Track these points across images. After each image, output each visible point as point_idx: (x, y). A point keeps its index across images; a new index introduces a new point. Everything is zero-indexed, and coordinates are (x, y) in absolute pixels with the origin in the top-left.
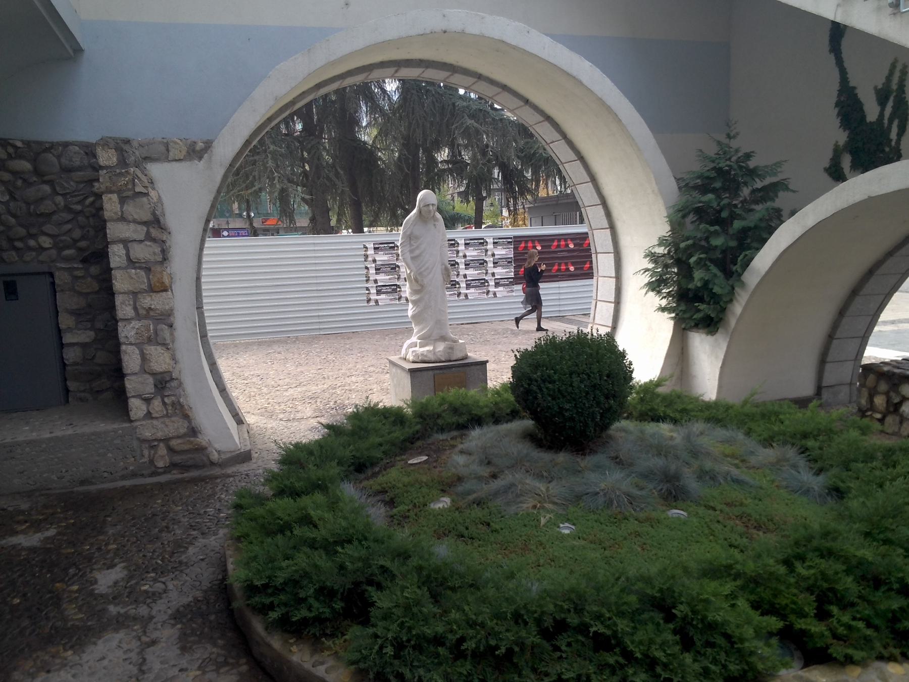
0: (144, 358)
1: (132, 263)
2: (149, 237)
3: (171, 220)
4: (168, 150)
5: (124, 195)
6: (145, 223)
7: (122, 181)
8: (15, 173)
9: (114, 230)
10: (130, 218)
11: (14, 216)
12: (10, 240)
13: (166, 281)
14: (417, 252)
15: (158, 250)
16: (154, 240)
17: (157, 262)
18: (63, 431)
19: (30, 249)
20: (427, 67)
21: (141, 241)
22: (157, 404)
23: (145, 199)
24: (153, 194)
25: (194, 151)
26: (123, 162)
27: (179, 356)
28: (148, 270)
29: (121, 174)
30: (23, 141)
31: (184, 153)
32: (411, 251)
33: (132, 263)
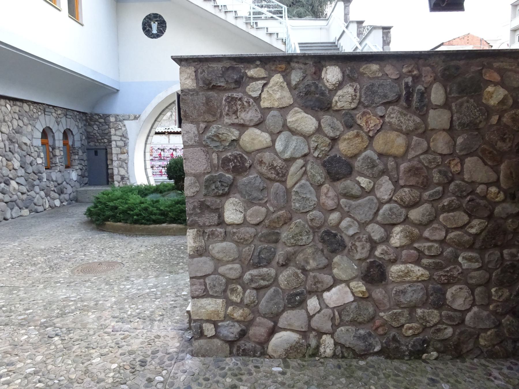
0: (119, 171)
1: (117, 146)
2: (121, 140)
3: (129, 136)
7: (116, 125)
8: (100, 123)
9: (113, 138)
12: (98, 140)
13: (125, 151)
15: (123, 143)
18: (98, 188)
19: (102, 142)
22: (121, 183)
24: (123, 129)
26: (116, 121)
27: (129, 171)
28: (121, 148)
33: (117, 146)
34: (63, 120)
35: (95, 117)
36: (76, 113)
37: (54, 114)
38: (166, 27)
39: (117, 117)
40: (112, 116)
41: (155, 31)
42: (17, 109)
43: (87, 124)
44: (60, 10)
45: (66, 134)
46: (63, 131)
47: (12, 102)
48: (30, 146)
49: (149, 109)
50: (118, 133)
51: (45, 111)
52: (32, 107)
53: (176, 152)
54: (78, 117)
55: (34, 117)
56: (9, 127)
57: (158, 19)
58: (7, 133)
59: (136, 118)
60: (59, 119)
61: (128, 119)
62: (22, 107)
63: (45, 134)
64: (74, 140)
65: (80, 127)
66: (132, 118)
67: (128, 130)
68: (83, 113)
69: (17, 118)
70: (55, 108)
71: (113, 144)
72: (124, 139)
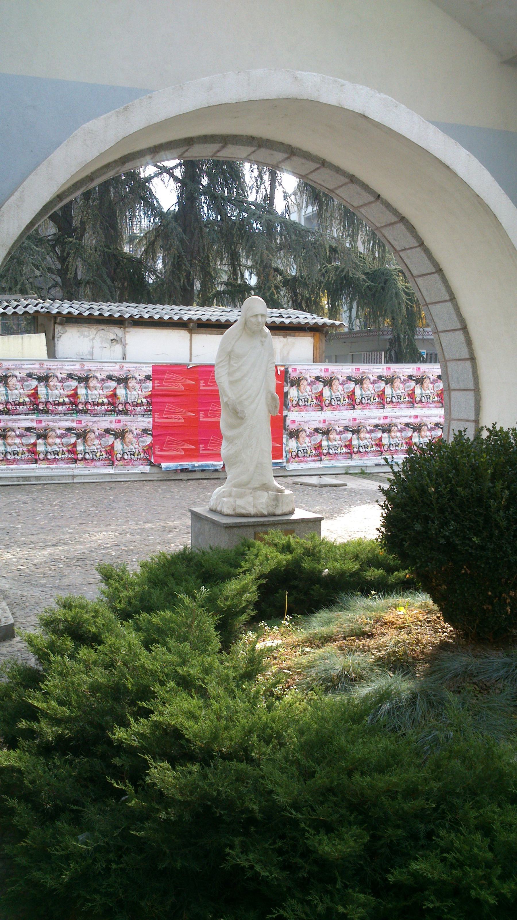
20: (259, 146)
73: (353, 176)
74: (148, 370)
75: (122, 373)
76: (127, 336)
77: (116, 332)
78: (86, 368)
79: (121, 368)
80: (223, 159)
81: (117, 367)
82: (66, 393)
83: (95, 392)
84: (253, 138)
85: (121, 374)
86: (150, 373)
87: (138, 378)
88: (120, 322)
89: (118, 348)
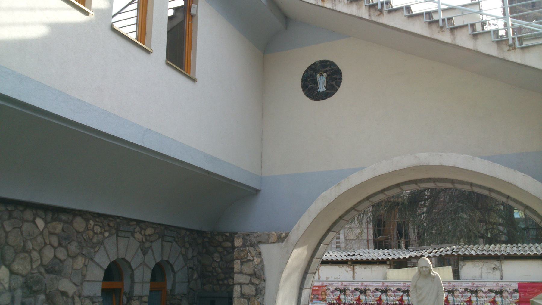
1: (243, 295)
2: (251, 282)
4: (269, 238)
5: (243, 260)
6: (250, 275)
7: (243, 254)
8: (225, 248)
9: (238, 278)
10: (244, 272)
11: (221, 269)
14: (421, 298)
16: (253, 284)
17: (253, 295)
21: (247, 284)
23: (251, 263)
24: (256, 260)
25: (280, 238)
26: (244, 245)
28: (249, 300)
29: (243, 251)
30: (229, 233)
31: (276, 239)
32: (417, 297)
33: (243, 295)
34: (157, 246)
35: (217, 238)
36: (183, 232)
37: (138, 236)
38: (341, 79)
39: (247, 238)
40: (239, 237)
41: (322, 88)
42: (59, 227)
43: (204, 251)
44: (148, 52)
45: (159, 272)
46: (152, 265)
47: (50, 216)
48: (73, 298)
49: (305, 221)
50: (248, 269)
51: (118, 230)
52: (92, 222)
53: (365, 295)
54: (186, 239)
55: (95, 241)
56: (32, 261)
57: (328, 68)
58: (24, 273)
59: (281, 239)
60: (147, 245)
61: (267, 242)
62: (71, 223)
63: (114, 272)
64: (174, 281)
65: (190, 256)
66: (273, 238)
67: (266, 263)
68: (198, 232)
69: (56, 244)
70: (142, 225)
71: (237, 288)
72: (257, 282)
73: (490, 188)
74: (516, 286)
75: (498, 288)
76: (503, 265)
77: (494, 263)
78: (475, 285)
79: (497, 285)
80: (432, 185)
81: (495, 284)
82: (464, 300)
83: (482, 299)
84: (430, 179)
85: (498, 289)
86: (517, 288)
87: (509, 291)
88: (497, 258)
89: (498, 273)
